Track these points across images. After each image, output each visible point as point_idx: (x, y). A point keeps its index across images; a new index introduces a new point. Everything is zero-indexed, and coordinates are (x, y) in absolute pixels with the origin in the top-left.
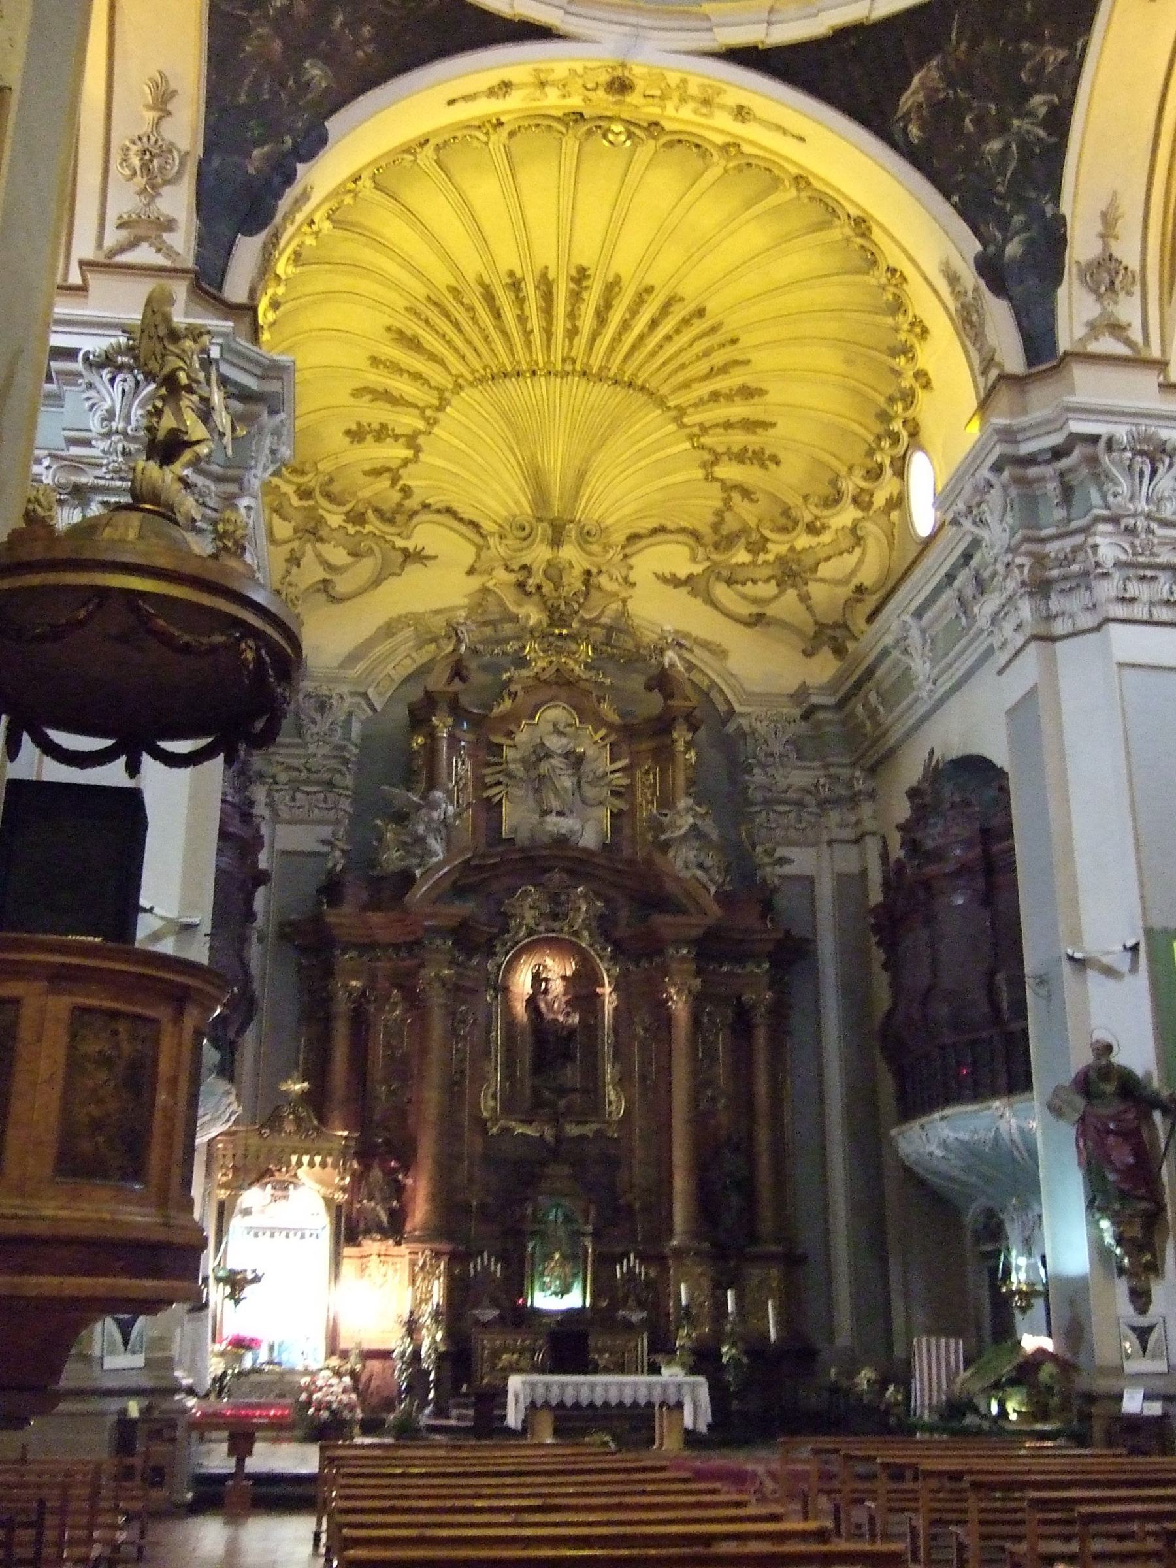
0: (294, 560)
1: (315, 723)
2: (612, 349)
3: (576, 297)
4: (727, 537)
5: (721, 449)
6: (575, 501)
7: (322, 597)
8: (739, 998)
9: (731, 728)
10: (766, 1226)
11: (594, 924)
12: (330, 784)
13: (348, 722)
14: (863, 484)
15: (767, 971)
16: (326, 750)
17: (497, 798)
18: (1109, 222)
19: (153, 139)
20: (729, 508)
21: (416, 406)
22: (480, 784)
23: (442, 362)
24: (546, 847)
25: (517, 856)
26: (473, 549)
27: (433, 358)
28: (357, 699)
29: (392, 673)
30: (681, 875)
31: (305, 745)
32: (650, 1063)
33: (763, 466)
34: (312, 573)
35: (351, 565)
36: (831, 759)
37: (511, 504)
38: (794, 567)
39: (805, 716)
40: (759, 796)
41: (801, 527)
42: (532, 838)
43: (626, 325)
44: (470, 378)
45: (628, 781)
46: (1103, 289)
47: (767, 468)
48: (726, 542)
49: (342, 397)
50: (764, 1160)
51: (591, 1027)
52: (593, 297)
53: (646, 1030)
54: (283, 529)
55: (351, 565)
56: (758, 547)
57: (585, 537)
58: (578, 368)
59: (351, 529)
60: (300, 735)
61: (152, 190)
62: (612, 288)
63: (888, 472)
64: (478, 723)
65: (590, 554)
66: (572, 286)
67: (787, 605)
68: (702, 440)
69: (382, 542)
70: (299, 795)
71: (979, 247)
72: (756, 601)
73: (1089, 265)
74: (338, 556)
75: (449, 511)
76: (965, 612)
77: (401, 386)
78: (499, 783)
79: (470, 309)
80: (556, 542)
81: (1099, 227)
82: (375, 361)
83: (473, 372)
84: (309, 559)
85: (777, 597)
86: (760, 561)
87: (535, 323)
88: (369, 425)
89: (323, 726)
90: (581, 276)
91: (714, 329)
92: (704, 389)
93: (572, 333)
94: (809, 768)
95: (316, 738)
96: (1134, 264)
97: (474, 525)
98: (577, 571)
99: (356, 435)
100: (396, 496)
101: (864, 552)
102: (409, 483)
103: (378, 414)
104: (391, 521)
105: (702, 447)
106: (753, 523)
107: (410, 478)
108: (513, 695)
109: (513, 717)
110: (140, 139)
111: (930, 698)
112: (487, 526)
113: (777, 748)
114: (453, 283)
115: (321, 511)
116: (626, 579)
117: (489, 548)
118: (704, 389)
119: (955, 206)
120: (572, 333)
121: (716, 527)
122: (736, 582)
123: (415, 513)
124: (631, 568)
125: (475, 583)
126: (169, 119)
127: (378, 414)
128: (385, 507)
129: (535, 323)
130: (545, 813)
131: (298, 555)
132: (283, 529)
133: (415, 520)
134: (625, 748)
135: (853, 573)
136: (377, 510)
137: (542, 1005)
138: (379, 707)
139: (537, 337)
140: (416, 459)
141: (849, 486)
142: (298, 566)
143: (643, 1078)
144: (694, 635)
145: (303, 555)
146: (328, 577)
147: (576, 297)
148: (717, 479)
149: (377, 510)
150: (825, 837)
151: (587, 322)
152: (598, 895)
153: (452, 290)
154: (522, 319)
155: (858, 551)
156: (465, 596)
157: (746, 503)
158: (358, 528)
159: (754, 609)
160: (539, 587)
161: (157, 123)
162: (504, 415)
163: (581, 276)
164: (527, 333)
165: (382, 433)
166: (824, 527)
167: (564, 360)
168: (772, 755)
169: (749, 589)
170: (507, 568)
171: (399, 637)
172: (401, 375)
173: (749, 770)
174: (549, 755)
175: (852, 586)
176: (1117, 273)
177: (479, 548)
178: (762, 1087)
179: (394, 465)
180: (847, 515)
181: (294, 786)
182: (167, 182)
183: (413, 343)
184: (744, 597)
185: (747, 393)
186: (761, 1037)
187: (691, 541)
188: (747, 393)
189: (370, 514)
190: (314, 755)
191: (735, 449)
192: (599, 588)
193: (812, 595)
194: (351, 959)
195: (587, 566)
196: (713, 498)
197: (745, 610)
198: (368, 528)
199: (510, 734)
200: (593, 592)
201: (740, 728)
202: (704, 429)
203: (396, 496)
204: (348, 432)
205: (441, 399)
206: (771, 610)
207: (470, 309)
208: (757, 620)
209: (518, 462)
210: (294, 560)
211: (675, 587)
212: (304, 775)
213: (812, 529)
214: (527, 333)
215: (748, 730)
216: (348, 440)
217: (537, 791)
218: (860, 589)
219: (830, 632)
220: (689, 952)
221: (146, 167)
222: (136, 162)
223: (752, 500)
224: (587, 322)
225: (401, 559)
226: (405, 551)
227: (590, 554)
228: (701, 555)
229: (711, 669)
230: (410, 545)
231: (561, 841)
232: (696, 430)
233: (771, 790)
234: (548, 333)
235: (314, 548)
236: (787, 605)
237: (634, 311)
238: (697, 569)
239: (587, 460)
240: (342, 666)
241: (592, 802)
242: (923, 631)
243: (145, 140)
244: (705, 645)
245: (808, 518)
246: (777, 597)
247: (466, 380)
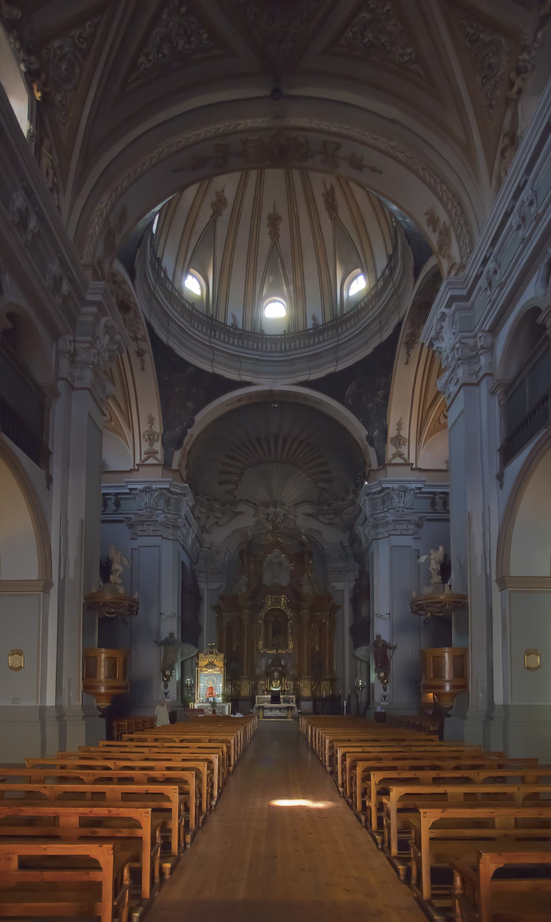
0: (208, 517)
18: (399, 426)
19: (150, 431)
46: (397, 444)
54: (204, 510)
56: (330, 505)
59: (222, 508)
61: (151, 444)
71: (367, 433)
73: (394, 438)
74: (219, 515)
75: (248, 501)
80: (275, 507)
81: (396, 427)
96: (407, 437)
97: (254, 504)
99: (221, 483)
110: (147, 431)
116: (295, 515)
119: (361, 422)
124: (296, 512)
126: (154, 425)
132: (204, 510)
138: (232, 553)
146: (217, 521)
155: (354, 507)
160: (272, 519)
161: (151, 427)
165: (227, 482)
176: (401, 440)
182: (154, 442)
195: (285, 512)
208: (330, 524)
210: (208, 517)
221: (149, 438)
222: (147, 437)
226: (236, 512)
238: (314, 511)
243: (148, 431)
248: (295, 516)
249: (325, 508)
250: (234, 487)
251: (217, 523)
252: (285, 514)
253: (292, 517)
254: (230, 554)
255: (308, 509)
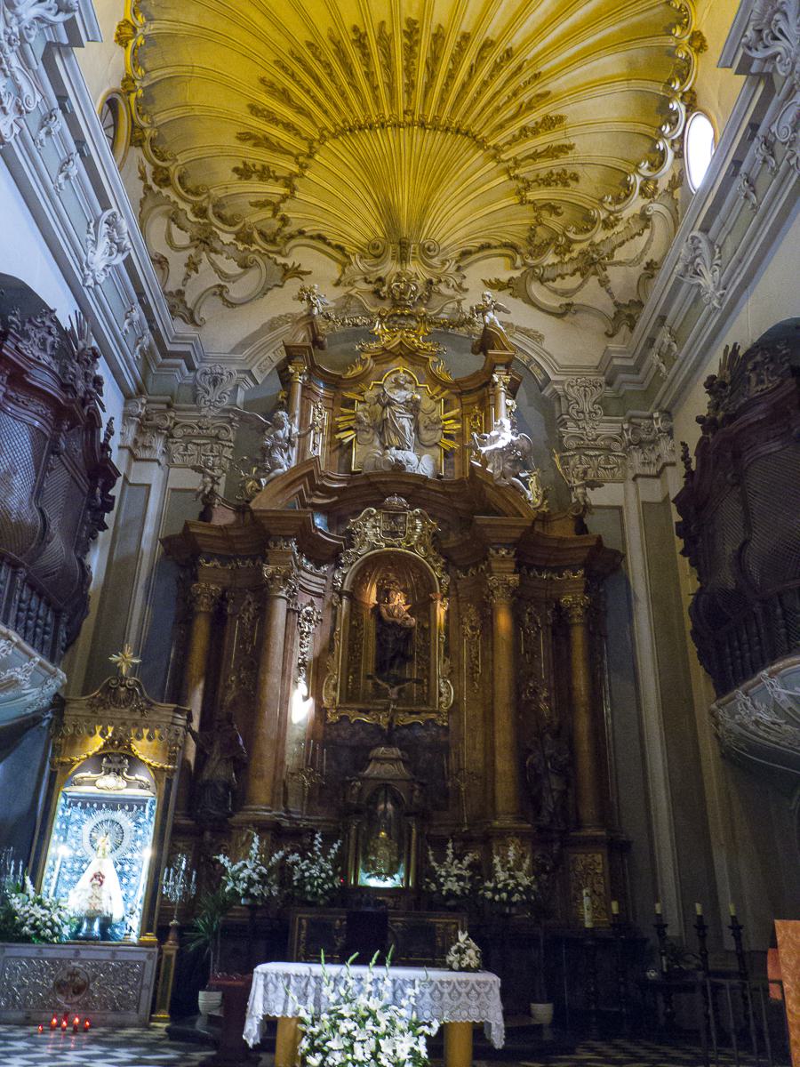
1: (207, 392)
2: (442, 100)
3: (410, 51)
4: (539, 246)
5: (531, 177)
6: (419, 231)
7: (218, 300)
8: (557, 602)
9: (547, 392)
10: (588, 811)
11: (428, 541)
12: (217, 437)
13: (235, 391)
14: (648, 174)
15: (584, 576)
16: (215, 412)
17: (346, 441)
20: (540, 224)
21: (290, 153)
22: (334, 429)
23: (309, 115)
24: (385, 474)
25: (363, 482)
26: (340, 267)
27: (301, 110)
28: (243, 376)
29: (272, 356)
30: (498, 483)
31: (199, 410)
32: (477, 658)
33: (566, 184)
34: (206, 278)
35: (240, 275)
36: (631, 412)
37: (370, 234)
38: (595, 256)
39: (609, 383)
40: (573, 444)
41: (599, 225)
42: (375, 467)
43: (451, 76)
44: (333, 130)
45: (459, 426)
47: (569, 186)
48: (540, 250)
49: (229, 139)
50: (584, 747)
51: (426, 632)
52: (424, 50)
53: (473, 628)
54: (181, 238)
55: (240, 275)
57: (426, 251)
58: (416, 118)
59: (241, 247)
60: (195, 400)
62: (438, 38)
63: (670, 155)
64: (334, 383)
65: (429, 266)
66: (406, 41)
67: (591, 293)
68: (517, 172)
69: (265, 258)
70: (190, 446)
72: (564, 294)
75: (321, 238)
76: (754, 192)
77: (277, 133)
78: (350, 429)
79: (327, 65)
80: (403, 259)
82: (255, 110)
83: (335, 125)
84: (204, 265)
85: (581, 286)
86: (566, 260)
87: (380, 78)
88: (254, 166)
89: (214, 395)
90: (412, 31)
91: (520, 68)
92: (514, 128)
93: (410, 86)
94: (611, 422)
95: (208, 403)
97: (340, 248)
98: (420, 282)
99: (244, 173)
100: (278, 224)
101: (652, 234)
102: (289, 215)
103: (259, 156)
104: (273, 242)
105: (516, 177)
106: (558, 229)
107: (285, 209)
108: (363, 362)
109: (361, 378)
111: (721, 305)
112: (348, 248)
113: (587, 406)
114: (310, 39)
115: (214, 229)
116: (460, 285)
117: (351, 264)
118: (514, 128)
120: (410, 86)
121: (530, 240)
122: (548, 280)
123: (291, 237)
124: (465, 277)
125: (340, 292)
127: (259, 156)
128: (268, 232)
129: (380, 78)
130: (387, 448)
131: (195, 260)
132: (181, 238)
133: (293, 242)
134: (456, 402)
135: (644, 252)
136: (262, 234)
137: (384, 611)
138: (260, 382)
139: (382, 91)
140: (292, 196)
141: (636, 179)
142: (197, 272)
143: (472, 670)
144: (515, 324)
145: (200, 261)
147: (410, 51)
148: (530, 202)
149: (262, 234)
150: (631, 475)
151: (421, 77)
152: (432, 516)
153: (310, 45)
154: (369, 75)
155: (647, 232)
156: (334, 301)
157: (554, 217)
158: (246, 246)
159: (564, 301)
162: (363, 164)
163: (412, 31)
164: (375, 88)
165: (265, 174)
166: (617, 219)
167: (405, 112)
168: (583, 412)
169: (558, 284)
170: (366, 280)
171: (280, 330)
172: (277, 125)
173: (564, 425)
174: (390, 403)
175: (643, 264)
177: (344, 265)
178: (581, 682)
179: (275, 199)
180: (636, 204)
181: (188, 439)
183: (285, 96)
184: (555, 291)
185: (551, 123)
186: (578, 635)
187: (509, 252)
188: (551, 123)
189: (256, 235)
190: (205, 416)
191: (543, 174)
192: (439, 293)
193: (610, 278)
194: (215, 567)
196: (526, 216)
197: (554, 302)
198: (255, 247)
199: (361, 393)
200: (434, 296)
201: (555, 391)
202: (517, 163)
203: (278, 224)
204: (236, 170)
205: (311, 147)
206: (577, 299)
207: (327, 65)
209: (375, 202)
211: (500, 290)
212: (196, 431)
213: (607, 225)
214: (375, 88)
215: (561, 393)
216: (236, 176)
217: (381, 434)
218: (651, 266)
219: (627, 312)
220: (508, 553)
223: (558, 214)
224: (421, 77)
225: (281, 275)
226: (284, 265)
227: (429, 266)
228: (519, 262)
229: (530, 349)
230: (289, 262)
231: (398, 467)
232: (511, 164)
233: (583, 439)
234: (391, 87)
235: (209, 257)
236: (591, 293)
237: (456, 60)
238: (516, 274)
239: (428, 197)
240: (233, 351)
241: (427, 443)
242: (711, 243)
244: (525, 332)
245: (603, 215)
246: (581, 286)
247: (329, 132)
248: (461, 288)
249: (551, 258)
250: (283, 191)
251: (220, 291)
252: (430, 282)
253: (450, 292)
254: (252, 385)
255: (500, 269)
